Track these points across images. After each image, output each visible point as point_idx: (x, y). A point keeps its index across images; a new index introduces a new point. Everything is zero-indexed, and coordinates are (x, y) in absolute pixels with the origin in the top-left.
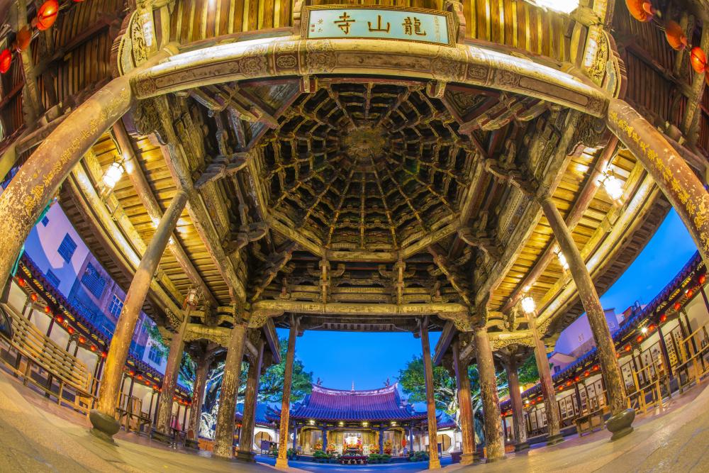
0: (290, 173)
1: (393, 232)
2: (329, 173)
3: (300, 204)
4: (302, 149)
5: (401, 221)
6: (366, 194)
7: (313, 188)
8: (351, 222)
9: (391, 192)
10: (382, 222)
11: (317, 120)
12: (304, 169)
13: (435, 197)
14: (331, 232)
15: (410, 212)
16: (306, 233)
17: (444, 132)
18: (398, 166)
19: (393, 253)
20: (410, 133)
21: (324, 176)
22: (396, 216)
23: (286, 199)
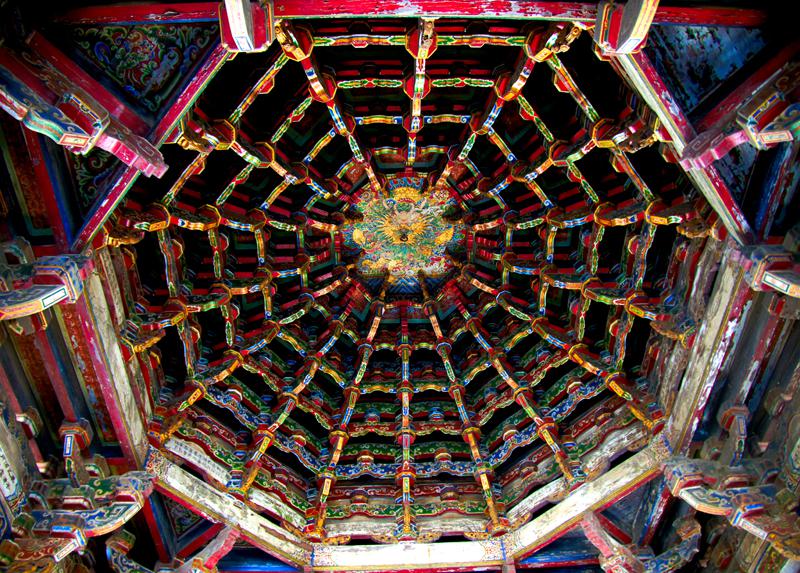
0: (211, 324)
1: (486, 485)
2: (315, 328)
3: (243, 417)
4: (242, 261)
5: (503, 454)
6: (412, 383)
7: (274, 370)
8: (378, 460)
9: (476, 371)
10: (455, 458)
11: (282, 172)
12: (251, 320)
13: (588, 378)
14: (326, 491)
15: (526, 424)
16: (259, 498)
17: (617, 194)
18: (489, 297)
19: (489, 544)
20: (519, 199)
21: (301, 338)
22: (488, 435)
23: (202, 403)
